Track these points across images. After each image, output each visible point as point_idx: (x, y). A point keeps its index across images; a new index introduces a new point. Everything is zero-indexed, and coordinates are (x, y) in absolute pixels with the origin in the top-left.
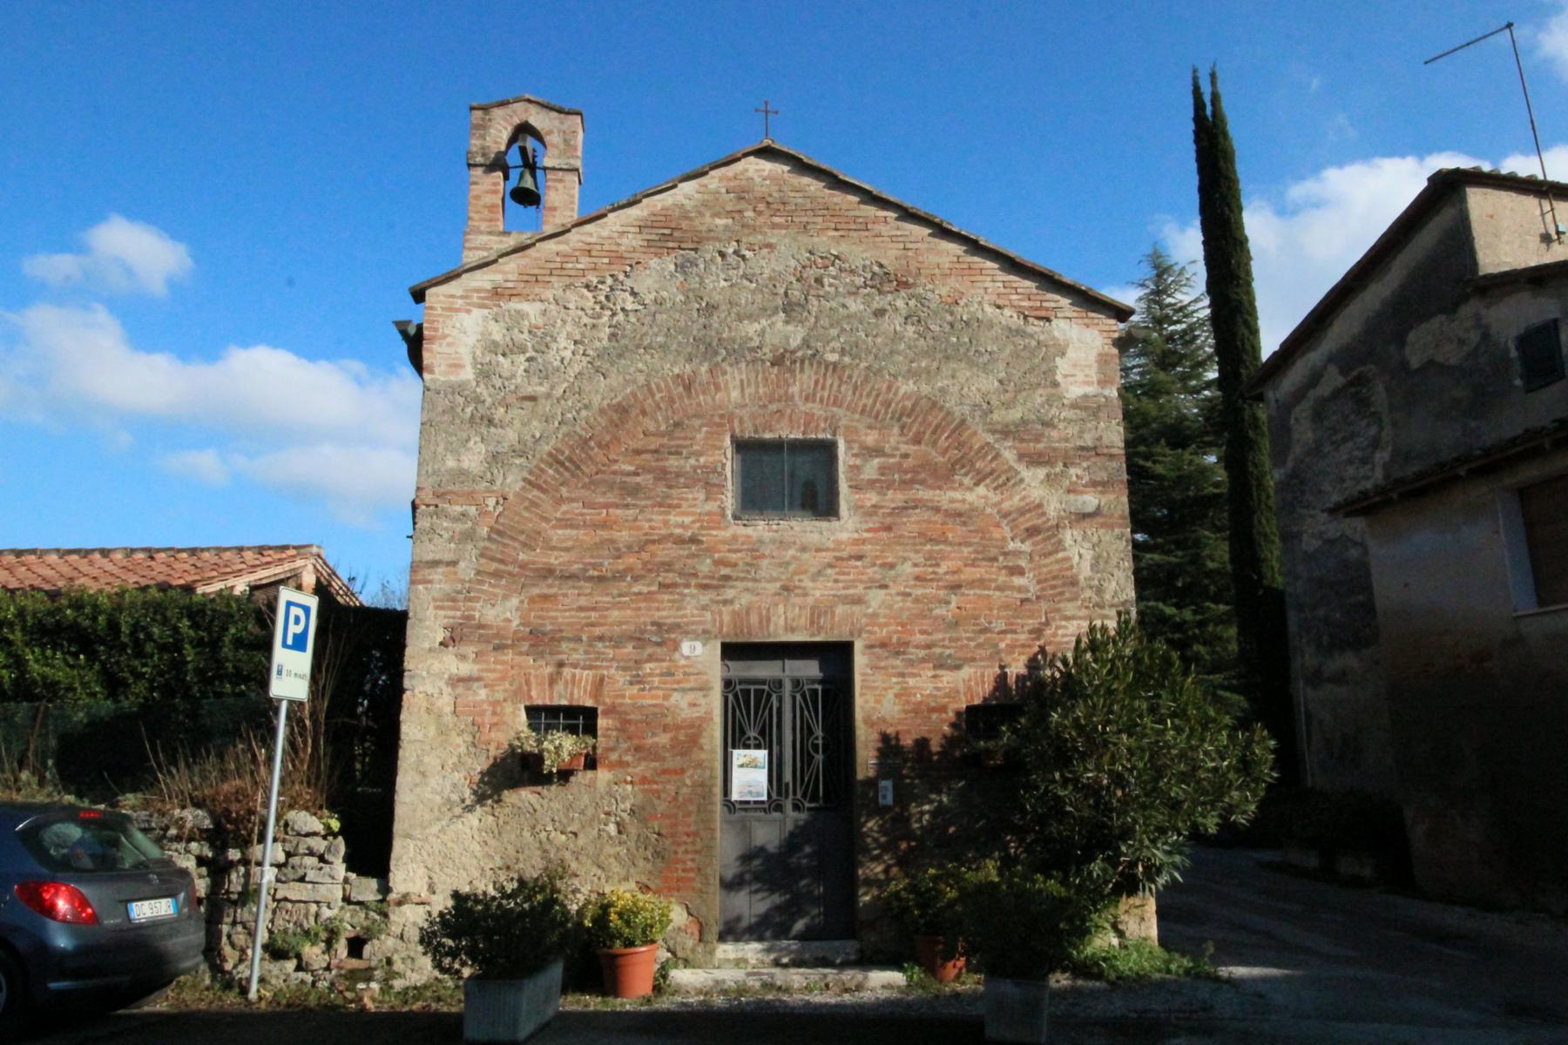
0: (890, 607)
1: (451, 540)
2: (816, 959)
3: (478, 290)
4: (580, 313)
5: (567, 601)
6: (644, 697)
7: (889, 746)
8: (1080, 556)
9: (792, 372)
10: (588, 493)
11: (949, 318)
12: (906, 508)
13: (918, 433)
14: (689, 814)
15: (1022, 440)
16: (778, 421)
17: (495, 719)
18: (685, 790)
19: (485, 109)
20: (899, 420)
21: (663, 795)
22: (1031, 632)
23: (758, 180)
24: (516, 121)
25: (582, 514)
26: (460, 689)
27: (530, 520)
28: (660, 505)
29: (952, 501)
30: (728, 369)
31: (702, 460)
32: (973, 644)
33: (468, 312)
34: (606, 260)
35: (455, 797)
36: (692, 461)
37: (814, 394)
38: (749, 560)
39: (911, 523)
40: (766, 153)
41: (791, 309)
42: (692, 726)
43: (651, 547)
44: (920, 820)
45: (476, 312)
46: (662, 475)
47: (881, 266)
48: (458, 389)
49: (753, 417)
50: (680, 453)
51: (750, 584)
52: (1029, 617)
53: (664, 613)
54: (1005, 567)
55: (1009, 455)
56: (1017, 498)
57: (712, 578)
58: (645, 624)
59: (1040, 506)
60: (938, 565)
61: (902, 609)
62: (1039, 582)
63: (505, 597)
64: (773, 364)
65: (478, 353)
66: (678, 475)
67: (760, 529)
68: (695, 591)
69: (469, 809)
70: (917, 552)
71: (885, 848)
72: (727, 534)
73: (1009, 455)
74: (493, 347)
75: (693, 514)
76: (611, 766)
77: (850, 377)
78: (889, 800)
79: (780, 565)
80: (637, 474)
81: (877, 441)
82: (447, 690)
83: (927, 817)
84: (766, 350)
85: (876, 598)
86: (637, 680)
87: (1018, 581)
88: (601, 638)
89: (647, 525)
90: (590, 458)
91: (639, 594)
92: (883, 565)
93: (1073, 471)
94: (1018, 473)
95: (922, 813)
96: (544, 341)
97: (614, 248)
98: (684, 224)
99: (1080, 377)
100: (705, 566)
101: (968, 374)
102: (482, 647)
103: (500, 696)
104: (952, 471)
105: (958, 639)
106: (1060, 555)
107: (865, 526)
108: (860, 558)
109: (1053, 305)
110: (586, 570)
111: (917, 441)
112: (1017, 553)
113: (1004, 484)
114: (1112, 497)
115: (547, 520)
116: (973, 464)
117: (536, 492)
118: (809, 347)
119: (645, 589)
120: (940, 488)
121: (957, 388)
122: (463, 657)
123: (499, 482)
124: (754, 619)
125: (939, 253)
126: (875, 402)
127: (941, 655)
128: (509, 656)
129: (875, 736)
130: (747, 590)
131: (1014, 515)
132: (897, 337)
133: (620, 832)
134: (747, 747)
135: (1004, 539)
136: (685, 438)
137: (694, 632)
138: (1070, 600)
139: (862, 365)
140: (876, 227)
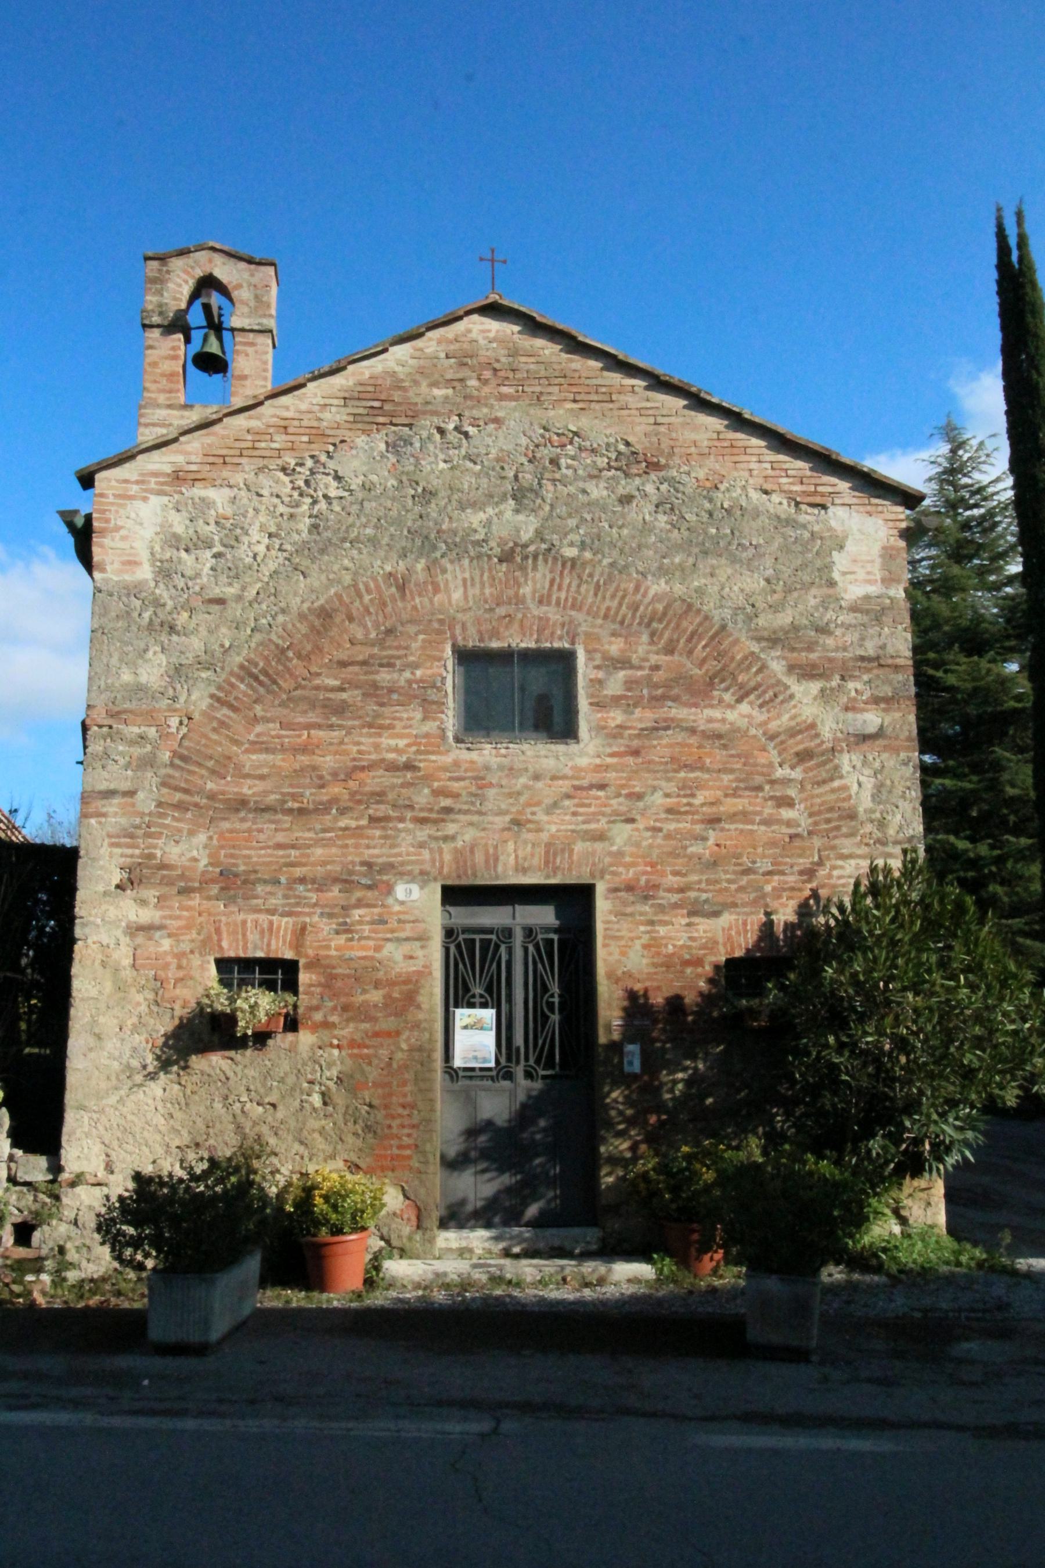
0: (638, 845)
1: (127, 766)
2: (552, 1248)
3: (155, 474)
4: (276, 501)
5: (262, 837)
6: (352, 948)
7: (636, 1005)
8: (860, 785)
9: (522, 568)
10: (285, 711)
11: (707, 505)
12: (657, 729)
13: (671, 640)
14: (404, 1083)
15: (793, 649)
16: (507, 627)
17: (181, 974)
18: (399, 1055)
19: (162, 259)
20: (648, 625)
21: (375, 1062)
22: (801, 873)
23: (482, 342)
24: (199, 273)
25: (279, 737)
26: (140, 939)
27: (220, 744)
28: (370, 726)
29: (710, 720)
30: (449, 566)
31: (418, 673)
32: (733, 887)
33: (145, 499)
34: (305, 439)
35: (135, 1063)
36: (407, 674)
37: (549, 596)
38: (473, 789)
39: (662, 747)
40: (493, 310)
41: (521, 496)
43: (362, 775)
44: (671, 1091)
45: (155, 500)
46: (372, 690)
47: (628, 444)
48: (134, 590)
49: (478, 621)
50: (390, 665)
51: (475, 818)
52: (800, 856)
53: (376, 851)
54: (772, 798)
55: (777, 667)
56: (785, 717)
57: (431, 810)
58: (353, 863)
59: (813, 726)
60: (693, 795)
61: (651, 846)
62: (811, 815)
63: (191, 833)
64: (500, 561)
65: (157, 548)
66: (391, 691)
67: (487, 753)
68: (411, 826)
69: (152, 1076)
70: (669, 780)
71: (631, 1122)
72: (448, 759)
73: (777, 667)
74: (174, 541)
75: (408, 736)
76: (315, 1028)
77: (591, 575)
78: (636, 1067)
79: (510, 795)
80: (342, 689)
81: (622, 651)
82: (125, 940)
83: (680, 1086)
84: (493, 544)
85: (621, 834)
86: (345, 929)
87: (787, 814)
88: (302, 880)
89: (355, 749)
90: (288, 670)
91: (346, 829)
92: (630, 796)
93: (851, 685)
94: (787, 687)
95: (675, 1082)
96: (233, 533)
97: (315, 424)
98: (397, 396)
99: (861, 575)
100: (422, 797)
101: (729, 571)
102: (165, 890)
103: (186, 947)
104: (711, 684)
105: (717, 882)
106: (836, 784)
107: (609, 750)
108: (602, 787)
109: (830, 489)
110: (285, 802)
111: (670, 650)
112: (786, 782)
113: (771, 700)
114: (898, 715)
115: (237, 743)
116: (735, 678)
117: (225, 711)
118: (543, 540)
119: (353, 824)
120: (696, 705)
121: (716, 588)
122: (143, 902)
123: (182, 700)
124: (479, 857)
125: (696, 428)
126: (620, 604)
127: (696, 900)
128: (196, 900)
129: (620, 993)
130: (471, 824)
131: (782, 737)
132: (646, 528)
133: (325, 1104)
134: (471, 1005)
135: (771, 765)
136: (398, 648)
138: (847, 836)
139: (605, 562)
140: (622, 397)
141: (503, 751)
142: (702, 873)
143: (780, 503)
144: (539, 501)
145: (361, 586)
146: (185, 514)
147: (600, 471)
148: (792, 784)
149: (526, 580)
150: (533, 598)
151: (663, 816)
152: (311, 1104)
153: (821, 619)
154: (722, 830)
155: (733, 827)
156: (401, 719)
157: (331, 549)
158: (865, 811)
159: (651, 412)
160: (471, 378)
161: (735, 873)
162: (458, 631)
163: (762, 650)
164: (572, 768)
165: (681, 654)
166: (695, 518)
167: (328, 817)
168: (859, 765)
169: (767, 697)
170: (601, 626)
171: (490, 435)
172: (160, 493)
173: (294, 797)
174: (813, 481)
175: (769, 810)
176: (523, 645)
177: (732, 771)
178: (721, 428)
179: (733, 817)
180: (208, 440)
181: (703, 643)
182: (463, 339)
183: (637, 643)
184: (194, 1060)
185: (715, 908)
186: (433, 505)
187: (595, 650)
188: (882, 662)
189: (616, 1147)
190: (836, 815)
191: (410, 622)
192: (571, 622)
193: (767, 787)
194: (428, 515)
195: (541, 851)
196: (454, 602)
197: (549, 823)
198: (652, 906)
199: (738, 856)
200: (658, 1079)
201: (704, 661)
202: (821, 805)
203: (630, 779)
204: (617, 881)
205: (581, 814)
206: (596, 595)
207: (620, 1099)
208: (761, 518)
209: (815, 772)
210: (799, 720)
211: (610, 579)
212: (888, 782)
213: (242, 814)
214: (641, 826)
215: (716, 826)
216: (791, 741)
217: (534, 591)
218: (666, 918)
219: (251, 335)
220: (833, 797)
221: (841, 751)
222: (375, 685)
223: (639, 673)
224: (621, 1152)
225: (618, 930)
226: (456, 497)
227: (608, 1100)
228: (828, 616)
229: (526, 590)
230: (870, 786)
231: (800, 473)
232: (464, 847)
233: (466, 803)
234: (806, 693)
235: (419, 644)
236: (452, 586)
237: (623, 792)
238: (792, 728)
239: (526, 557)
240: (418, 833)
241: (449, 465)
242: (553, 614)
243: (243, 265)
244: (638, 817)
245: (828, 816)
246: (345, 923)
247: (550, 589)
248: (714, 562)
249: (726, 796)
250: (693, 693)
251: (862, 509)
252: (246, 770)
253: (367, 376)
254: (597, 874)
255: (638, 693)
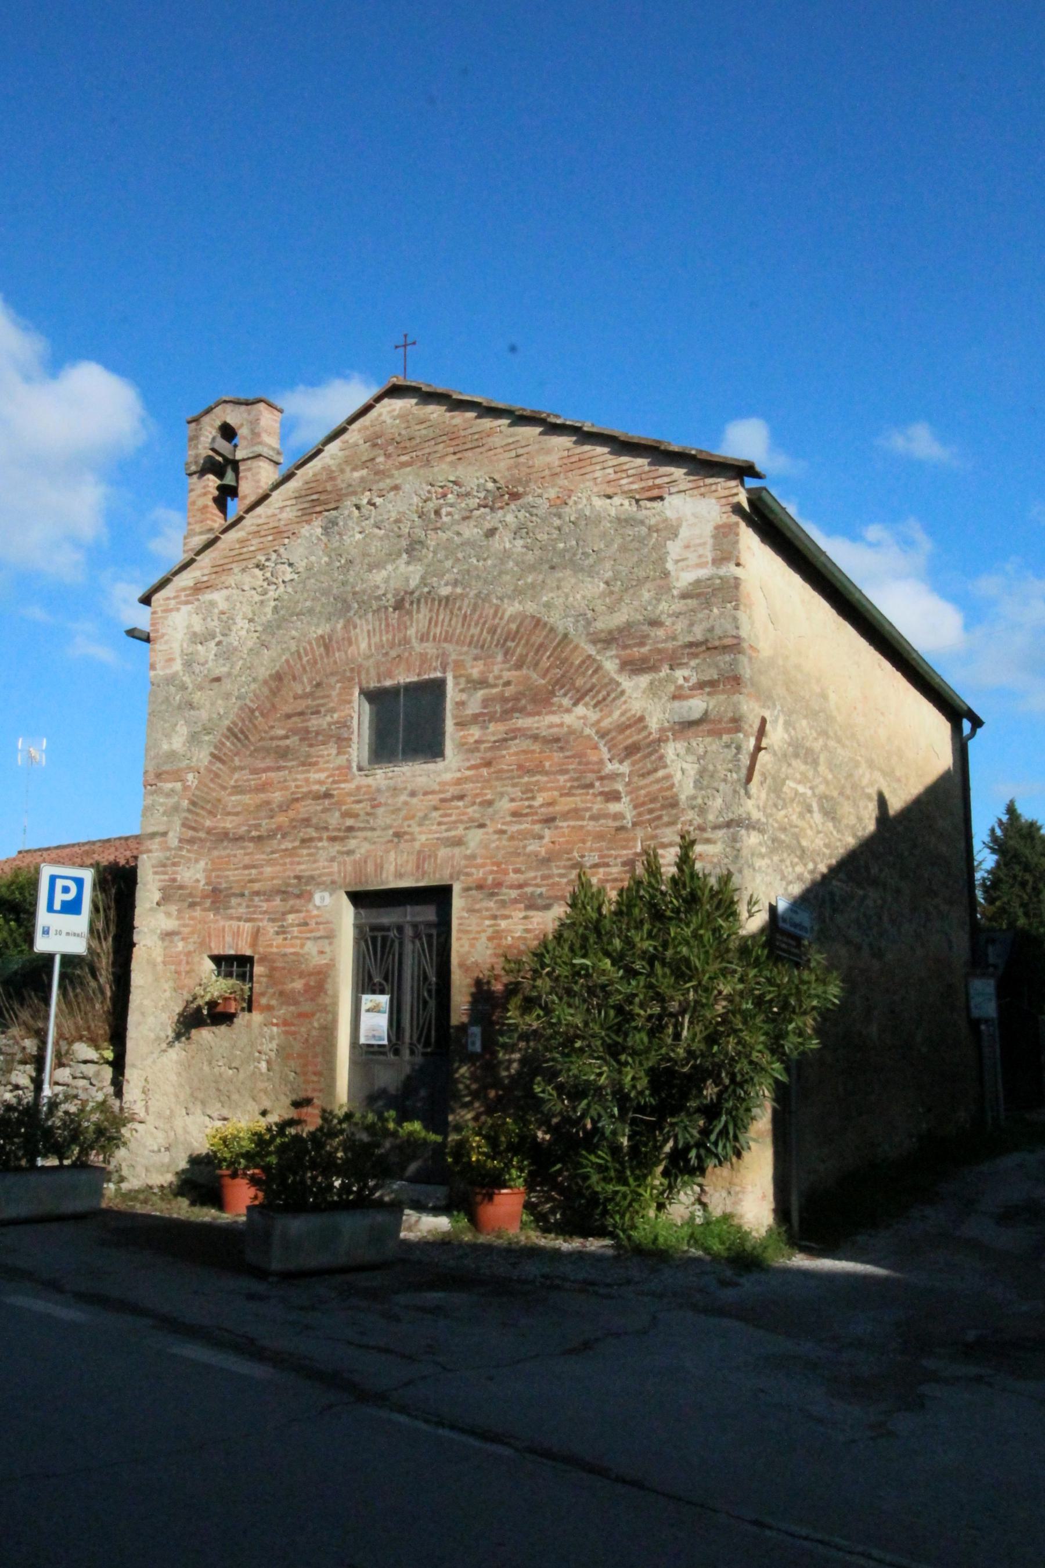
0: (486, 847)
1: (164, 813)
2: (412, 1201)
3: (184, 589)
4: (254, 592)
5: (236, 860)
6: (285, 946)
7: (481, 993)
8: (683, 771)
9: (409, 613)
11: (557, 522)
12: (505, 740)
13: (521, 656)
14: (315, 1056)
15: (625, 647)
16: (398, 665)
17: (188, 968)
18: (314, 1033)
19: (196, 420)
20: (503, 645)
21: (298, 1037)
22: (624, 864)
23: (389, 421)
24: (218, 423)
27: (213, 790)
28: (303, 764)
29: (551, 726)
30: (358, 622)
31: (336, 716)
32: (565, 880)
34: (270, 538)
35: (163, 1035)
36: (328, 719)
37: (428, 633)
38: (369, 809)
39: (509, 756)
40: (395, 391)
41: (413, 548)
42: (319, 973)
43: (297, 805)
44: (508, 1069)
45: (185, 609)
46: (305, 735)
47: (495, 481)
48: (171, 680)
49: (378, 665)
50: (318, 712)
51: (369, 834)
52: (624, 848)
53: (303, 867)
54: (601, 793)
55: (610, 666)
56: (617, 714)
57: (339, 830)
58: (289, 877)
59: (642, 719)
60: (533, 798)
61: (498, 848)
62: (635, 807)
63: (197, 861)
64: (395, 609)
65: (185, 645)
66: (317, 733)
67: (381, 777)
68: (325, 843)
69: (170, 1045)
70: (514, 785)
71: (475, 1095)
72: (352, 786)
73: (610, 666)
75: (327, 769)
77: (460, 609)
78: (478, 1048)
79: (393, 812)
80: (286, 737)
81: (482, 673)
83: (515, 1065)
84: (389, 596)
85: (475, 838)
86: (282, 931)
87: (614, 807)
88: (257, 893)
89: (293, 784)
90: (255, 726)
91: (286, 850)
92: (482, 804)
93: (680, 674)
94: (618, 684)
95: (510, 1061)
96: (227, 622)
97: (276, 525)
99: (693, 558)
100: (334, 819)
101: (573, 581)
103: (191, 948)
104: (552, 693)
105: (549, 877)
106: (661, 773)
107: (468, 764)
108: (461, 797)
109: (666, 479)
110: (249, 831)
111: (519, 666)
112: (614, 776)
113: (604, 699)
114: (722, 697)
115: (224, 788)
116: (573, 684)
118: (425, 585)
119: (290, 846)
120: (539, 714)
121: (561, 600)
123: (194, 759)
124: (370, 868)
125: (548, 452)
126: (482, 630)
127: (532, 894)
128: (198, 913)
129: (469, 981)
130: (365, 839)
131: (614, 734)
132: (507, 554)
133: (269, 1070)
134: (374, 992)
136: (323, 697)
137: (324, 883)
139: (472, 594)
141: (390, 774)
142: (537, 869)
143: (622, 505)
144: (425, 551)
145: (302, 651)
146: (201, 615)
147: (471, 511)
148: (619, 779)
149: (412, 622)
150: (416, 637)
151: (509, 819)
152: (259, 1069)
153: (653, 611)
154: (557, 828)
155: (565, 824)
156: (322, 756)
157: (284, 625)
158: (687, 797)
159: (512, 446)
160: (379, 455)
161: (565, 867)
162: (363, 676)
163: (598, 652)
164: (439, 784)
165: (528, 668)
166: (546, 537)
167: (275, 841)
168: (682, 752)
169: (600, 697)
170: (466, 653)
171: (390, 502)
172: (187, 603)
173: (257, 827)
174: (652, 475)
175: (598, 806)
176: (408, 680)
177: (565, 772)
178: (570, 445)
179: (566, 816)
180: (213, 555)
181: (548, 653)
182: (377, 423)
183: (493, 664)
184: (193, 1032)
185: (548, 901)
186: (351, 572)
187: (461, 676)
188: (710, 645)
189: (462, 1117)
190: (659, 805)
191: (332, 674)
192: (444, 654)
193: (597, 784)
194: (347, 581)
195: (414, 857)
196: (361, 651)
197: (420, 833)
198: (496, 902)
199: (569, 852)
200: (496, 1057)
201: (548, 670)
202: (645, 796)
203: (482, 789)
204: (470, 881)
205: (445, 824)
206: (463, 625)
207: (467, 1075)
208: (603, 523)
209: (641, 764)
210: (629, 715)
211: (475, 607)
212: (711, 767)
213: (225, 844)
214: (490, 830)
215: (552, 825)
216: (621, 737)
217: (417, 633)
218: (507, 912)
219: (249, 462)
220: (656, 787)
221: (667, 740)
222: (307, 731)
223: (494, 691)
224: (466, 1121)
225: (469, 926)
226: (366, 561)
227: (457, 1076)
228: (661, 608)
229: (411, 632)
230: (692, 773)
231: (639, 470)
232: (360, 859)
233: (363, 822)
234: (637, 687)
235: (337, 691)
236: (360, 638)
237: (478, 800)
238: (623, 723)
239: (412, 603)
240: (331, 850)
241: (363, 535)
242: (430, 648)
243: (243, 408)
244: (488, 822)
245: (652, 806)
246: (283, 926)
247: (429, 627)
248: (561, 575)
249: (562, 795)
250: (534, 700)
251: (695, 492)
252: (229, 809)
253: (311, 474)
254: (455, 877)
255: (492, 709)
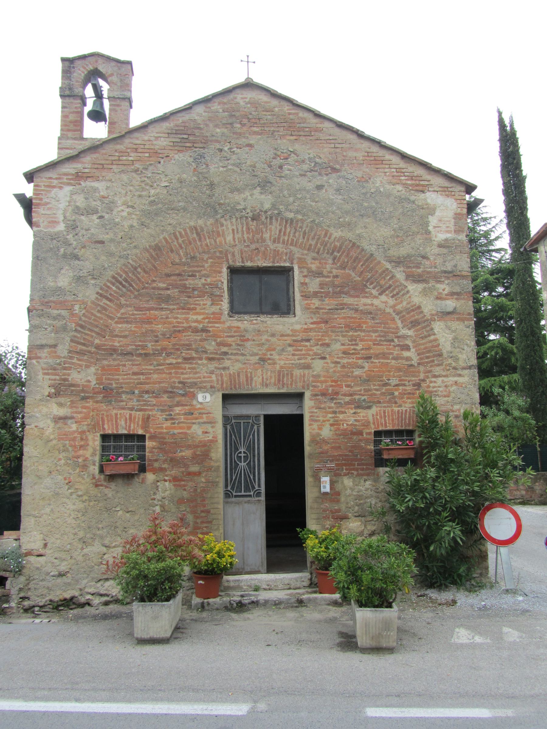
0: (328, 371)
6: (174, 428)
10: (137, 301)
17: (82, 443)
22: (414, 385)
23: (242, 103)
24: (91, 68)
25: (133, 314)
26: (60, 425)
27: (101, 319)
28: (183, 309)
30: (224, 222)
31: (209, 280)
33: (61, 188)
34: (147, 155)
36: (203, 280)
37: (279, 238)
38: (239, 342)
41: (264, 185)
42: (205, 446)
49: (242, 252)
50: (195, 276)
51: (240, 358)
52: (413, 376)
53: (186, 376)
54: (398, 345)
55: (400, 275)
56: (404, 303)
57: (216, 353)
58: (174, 382)
59: (419, 307)
60: (357, 345)
61: (334, 372)
62: (418, 355)
63: (87, 367)
66: (194, 289)
67: (246, 323)
68: (205, 361)
70: (343, 336)
73: (400, 275)
74: (77, 210)
76: (154, 471)
77: (301, 227)
79: (259, 345)
80: (168, 289)
82: (52, 425)
84: (248, 211)
85: (318, 366)
86: (170, 418)
87: (406, 354)
97: (152, 147)
98: (197, 132)
102: (73, 398)
105: (369, 390)
106: (432, 337)
108: (308, 340)
109: (426, 183)
112: (405, 337)
113: (398, 294)
115: (112, 318)
117: (105, 301)
119: (174, 361)
120: (357, 296)
122: (61, 405)
124: (243, 378)
126: (317, 243)
127: (359, 399)
128: (90, 404)
135: (397, 328)
136: (197, 266)
137: (205, 387)
138: (438, 365)
139: (309, 220)
140: (317, 134)
145: (178, 234)
149: (266, 231)
154: (372, 362)
159: (332, 141)
161: (379, 385)
162: (230, 257)
164: (292, 330)
167: (161, 358)
169: (395, 292)
172: (69, 184)
176: (265, 265)
177: (376, 331)
179: (377, 356)
183: (326, 263)
185: (369, 404)
192: (291, 252)
193: (396, 340)
197: (280, 360)
198: (335, 403)
202: (424, 349)
203: (323, 336)
205: (297, 355)
206: (304, 238)
211: (312, 229)
213: (115, 356)
215: (369, 361)
217: (270, 237)
220: (430, 344)
222: (184, 286)
223: (327, 280)
225: (317, 417)
233: (235, 349)
236: (226, 233)
237: (319, 343)
244: (327, 356)
246: (171, 415)
247: (279, 235)
249: (374, 344)
251: (444, 193)
252: (116, 333)
254: (306, 388)
